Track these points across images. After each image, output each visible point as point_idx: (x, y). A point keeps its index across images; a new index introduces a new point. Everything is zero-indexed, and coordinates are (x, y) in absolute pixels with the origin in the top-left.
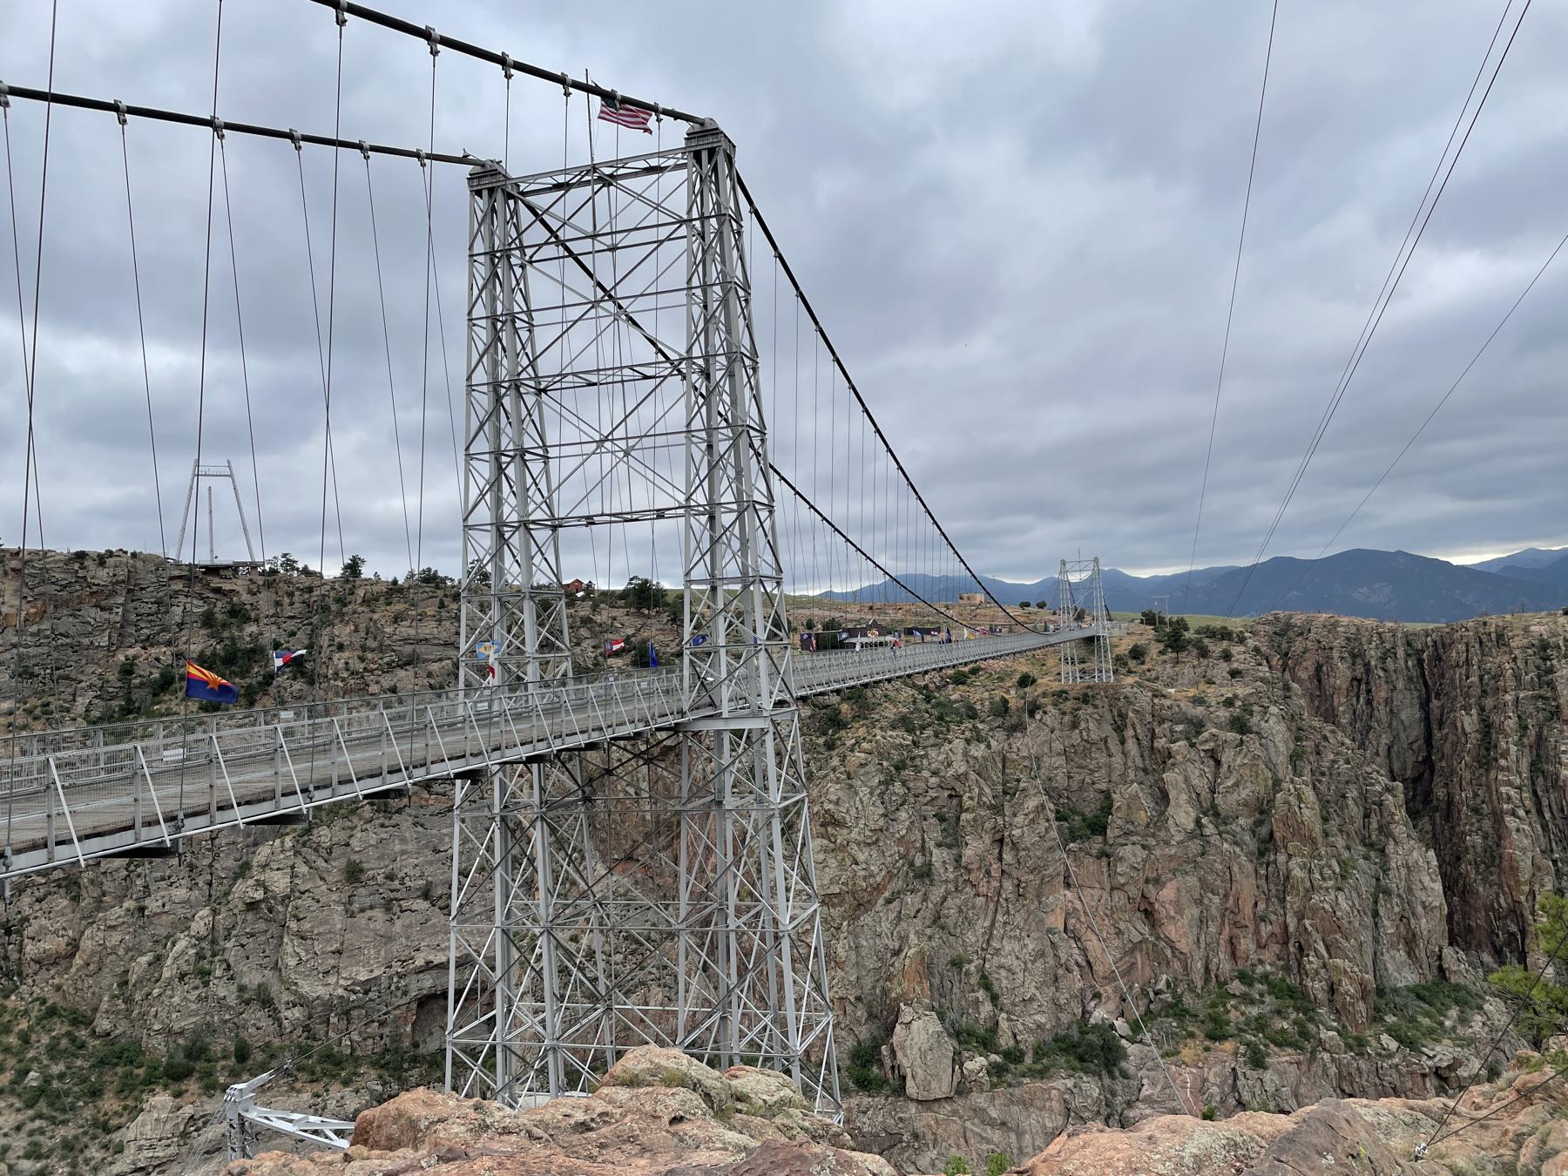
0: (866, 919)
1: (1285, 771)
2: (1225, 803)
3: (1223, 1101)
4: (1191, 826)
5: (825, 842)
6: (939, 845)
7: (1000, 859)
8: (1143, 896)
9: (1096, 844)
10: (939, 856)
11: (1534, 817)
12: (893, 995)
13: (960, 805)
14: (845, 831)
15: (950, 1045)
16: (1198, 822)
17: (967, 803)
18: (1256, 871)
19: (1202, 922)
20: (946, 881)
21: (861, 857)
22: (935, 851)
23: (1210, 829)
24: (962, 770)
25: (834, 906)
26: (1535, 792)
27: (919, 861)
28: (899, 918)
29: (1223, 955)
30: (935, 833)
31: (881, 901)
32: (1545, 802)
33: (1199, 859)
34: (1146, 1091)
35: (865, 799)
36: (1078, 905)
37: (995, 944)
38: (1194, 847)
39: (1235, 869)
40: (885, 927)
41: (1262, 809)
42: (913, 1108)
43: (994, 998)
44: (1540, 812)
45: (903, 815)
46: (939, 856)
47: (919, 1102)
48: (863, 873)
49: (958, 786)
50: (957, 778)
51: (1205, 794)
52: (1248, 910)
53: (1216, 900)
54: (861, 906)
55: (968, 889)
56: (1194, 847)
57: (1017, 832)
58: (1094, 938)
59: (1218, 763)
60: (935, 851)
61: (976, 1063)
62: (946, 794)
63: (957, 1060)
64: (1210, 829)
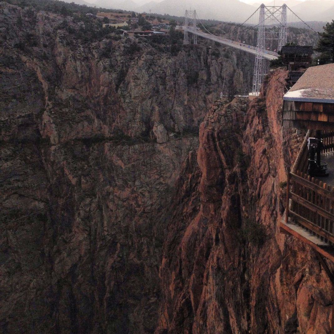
0: (144, 103)
1: (236, 68)
2: (224, 75)
4: (216, 80)
6: (161, 85)
9: (195, 85)
10: (161, 87)
12: (153, 120)
13: (165, 74)
15: (166, 131)
17: (167, 74)
23: (220, 82)
27: (156, 88)
28: (152, 102)
30: (159, 82)
40: (149, 104)
42: (158, 145)
43: (174, 121)
46: (161, 87)
47: (160, 144)
49: (165, 70)
50: (165, 68)
51: (219, 73)
54: (144, 99)
59: (222, 65)
61: (172, 135)
63: (168, 134)
64: (220, 82)
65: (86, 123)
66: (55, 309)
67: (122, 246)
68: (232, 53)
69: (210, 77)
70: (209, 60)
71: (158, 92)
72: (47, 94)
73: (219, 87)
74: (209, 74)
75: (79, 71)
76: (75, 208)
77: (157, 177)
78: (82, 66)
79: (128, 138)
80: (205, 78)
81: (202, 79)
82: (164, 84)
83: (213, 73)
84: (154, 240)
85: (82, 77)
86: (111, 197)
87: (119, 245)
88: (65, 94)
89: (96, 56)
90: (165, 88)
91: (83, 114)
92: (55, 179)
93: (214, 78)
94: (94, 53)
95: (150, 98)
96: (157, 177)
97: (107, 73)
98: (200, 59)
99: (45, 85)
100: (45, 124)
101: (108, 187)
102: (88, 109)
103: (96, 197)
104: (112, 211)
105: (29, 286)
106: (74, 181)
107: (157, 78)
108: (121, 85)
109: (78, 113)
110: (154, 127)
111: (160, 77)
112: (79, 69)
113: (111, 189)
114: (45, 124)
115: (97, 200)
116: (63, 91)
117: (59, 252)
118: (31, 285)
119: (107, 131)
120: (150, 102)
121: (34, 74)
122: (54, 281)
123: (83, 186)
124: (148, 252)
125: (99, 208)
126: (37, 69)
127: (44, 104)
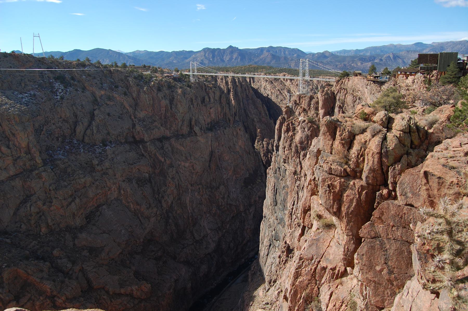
4: (213, 101)
16: (214, 101)
23: (215, 102)
38: (214, 104)
46: (192, 106)
56: (214, 104)
64: (215, 102)
65: (157, 130)
66: (168, 225)
67: (191, 190)
70: (207, 90)
72: (132, 115)
73: (215, 105)
74: (209, 98)
76: (166, 174)
77: (200, 154)
78: (149, 97)
79: (182, 135)
80: (208, 100)
81: (207, 101)
82: (192, 104)
83: (211, 97)
84: (204, 186)
85: (149, 103)
86: (180, 167)
87: (190, 190)
88: (142, 115)
89: (155, 91)
91: (154, 125)
92: (152, 160)
93: (212, 100)
96: (200, 154)
97: (164, 100)
98: (203, 89)
99: (130, 110)
100: (138, 131)
101: (178, 162)
102: (155, 122)
103: (174, 167)
104: (183, 173)
105: (156, 214)
106: (163, 160)
107: (188, 101)
108: (173, 106)
110: (194, 128)
111: (190, 101)
113: (180, 163)
114: (138, 131)
115: (175, 168)
116: (140, 113)
117: (163, 197)
118: (158, 213)
119: (168, 133)
121: (122, 104)
122: (164, 211)
123: (167, 162)
124: (203, 192)
125: (177, 172)
126: (123, 101)
127: (133, 121)
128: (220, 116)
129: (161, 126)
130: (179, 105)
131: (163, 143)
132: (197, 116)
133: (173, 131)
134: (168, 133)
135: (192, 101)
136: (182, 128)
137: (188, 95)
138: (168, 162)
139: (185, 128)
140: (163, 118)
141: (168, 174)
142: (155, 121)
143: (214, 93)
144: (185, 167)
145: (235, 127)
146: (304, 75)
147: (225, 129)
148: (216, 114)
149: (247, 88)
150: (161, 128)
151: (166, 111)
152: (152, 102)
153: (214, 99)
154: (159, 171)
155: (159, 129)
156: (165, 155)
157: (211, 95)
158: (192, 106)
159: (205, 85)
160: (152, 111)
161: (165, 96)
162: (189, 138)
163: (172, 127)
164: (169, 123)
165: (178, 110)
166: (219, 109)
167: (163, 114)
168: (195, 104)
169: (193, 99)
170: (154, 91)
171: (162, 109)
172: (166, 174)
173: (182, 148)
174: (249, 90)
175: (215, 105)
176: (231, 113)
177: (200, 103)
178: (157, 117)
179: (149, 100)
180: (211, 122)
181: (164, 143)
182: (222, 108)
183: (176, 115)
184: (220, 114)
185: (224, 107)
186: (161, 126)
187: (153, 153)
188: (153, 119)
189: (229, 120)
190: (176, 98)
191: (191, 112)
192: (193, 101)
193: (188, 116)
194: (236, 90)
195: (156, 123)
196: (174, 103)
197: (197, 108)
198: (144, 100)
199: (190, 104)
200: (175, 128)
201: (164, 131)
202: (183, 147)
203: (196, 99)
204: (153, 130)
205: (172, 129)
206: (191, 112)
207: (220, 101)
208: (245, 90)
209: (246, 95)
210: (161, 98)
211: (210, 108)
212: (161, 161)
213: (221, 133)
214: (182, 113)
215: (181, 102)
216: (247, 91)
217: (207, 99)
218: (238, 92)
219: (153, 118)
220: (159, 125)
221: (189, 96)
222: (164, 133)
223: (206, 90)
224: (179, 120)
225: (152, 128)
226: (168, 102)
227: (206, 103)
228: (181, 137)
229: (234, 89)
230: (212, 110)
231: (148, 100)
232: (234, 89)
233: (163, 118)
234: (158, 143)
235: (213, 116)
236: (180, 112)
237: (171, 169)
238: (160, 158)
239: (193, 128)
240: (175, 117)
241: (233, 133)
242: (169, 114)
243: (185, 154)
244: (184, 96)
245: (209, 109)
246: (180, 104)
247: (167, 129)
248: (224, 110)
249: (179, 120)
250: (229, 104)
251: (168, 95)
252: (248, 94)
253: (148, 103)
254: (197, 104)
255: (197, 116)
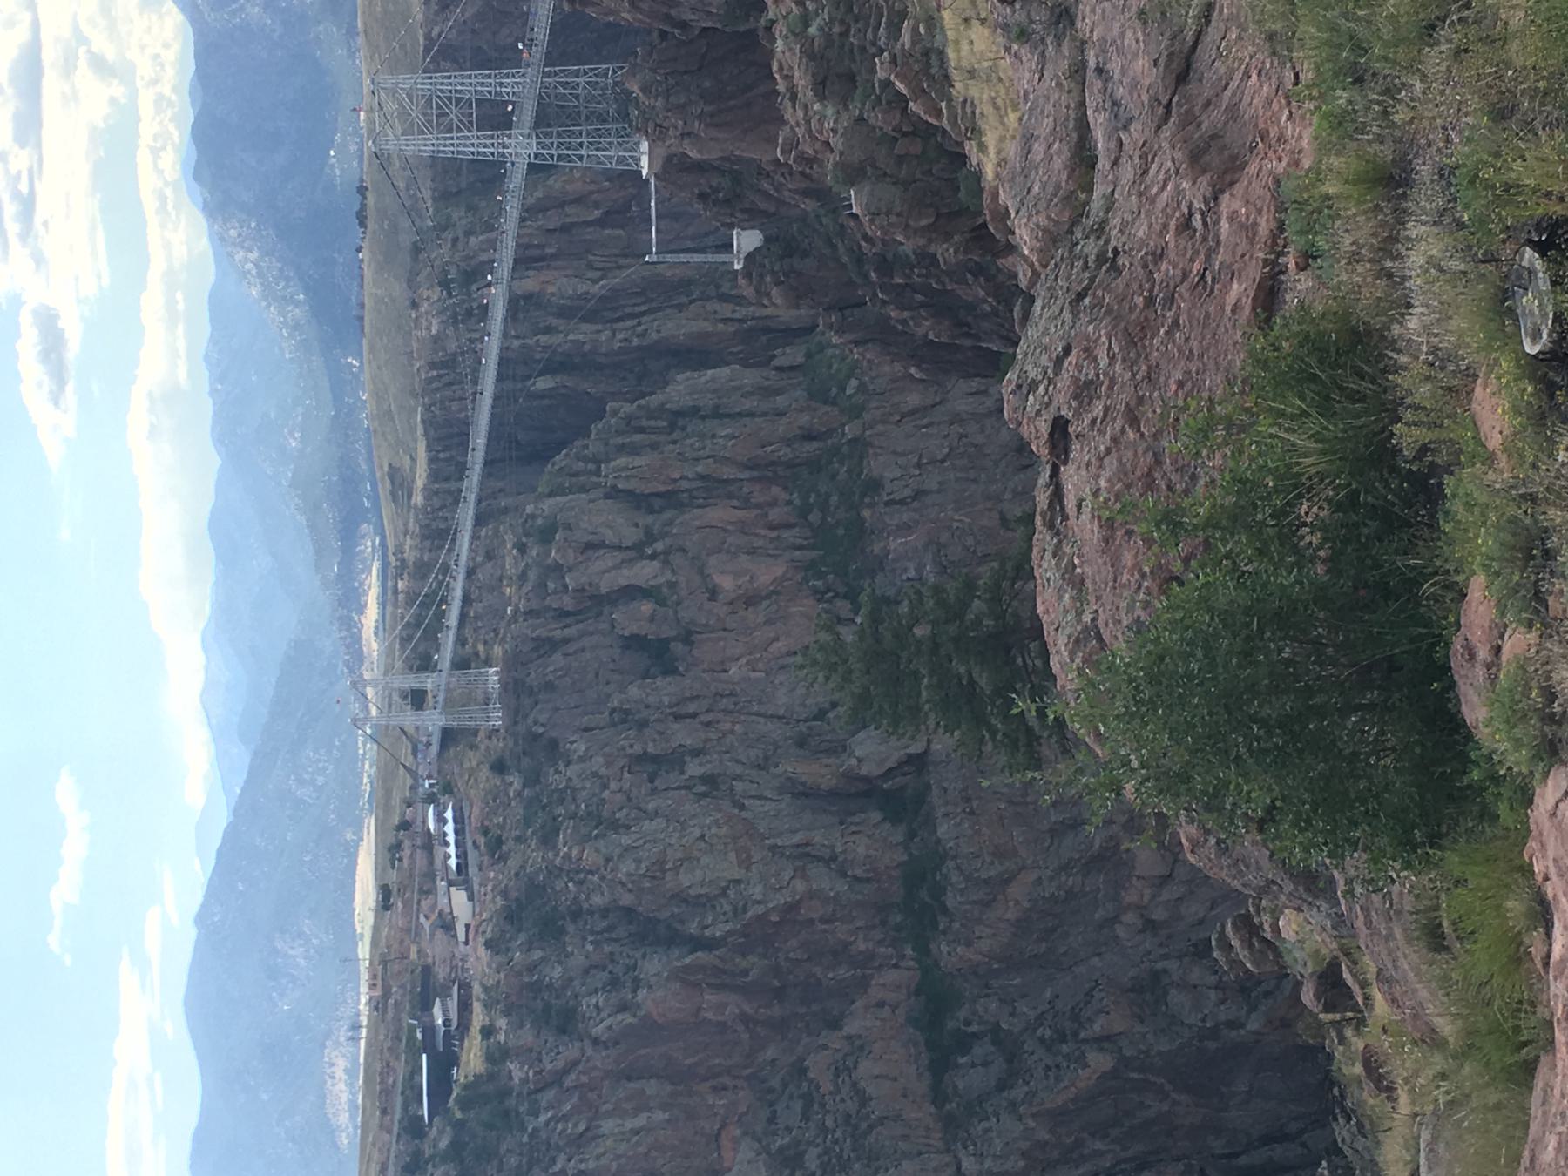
2: (631, 536)
3: (915, 510)
5: (682, 871)
6: (682, 773)
7: (694, 716)
8: (731, 603)
9: (678, 648)
11: (644, 319)
14: (669, 851)
16: (653, 557)
18: (699, 507)
19: (752, 552)
20: (721, 761)
21: (697, 833)
22: (689, 773)
24: (601, 760)
25: (749, 857)
26: (620, 319)
29: (786, 534)
31: (744, 814)
32: (628, 310)
33: (690, 554)
34: (912, 574)
35: (634, 837)
36: (743, 661)
37: (781, 712)
38: (677, 559)
39: (697, 523)
41: (639, 501)
44: (644, 313)
45: (651, 806)
46: (694, 769)
48: (713, 830)
52: (740, 514)
53: (730, 539)
55: (728, 741)
56: (677, 559)
57: (666, 700)
58: (776, 645)
60: (689, 773)
62: (626, 775)
64: (659, 546)
65: (866, 1067)
68: (533, 517)
69: (639, 589)
70: (567, 602)
71: (710, 780)
73: (683, 550)
74: (631, 593)
75: (641, 1120)
80: (647, 607)
81: (652, 619)
82: (674, 759)
83: (625, 577)
86: (1159, 914)
90: (697, 753)
91: (827, 1086)
92: (1099, 1145)
93: (645, 572)
94: (560, 1064)
95: (742, 807)
98: (566, 641)
101: (1120, 931)
102: (803, 1071)
103: (1165, 971)
106: (1099, 1062)
107: (654, 791)
108: (693, 928)
109: (823, 1105)
110: (864, 771)
111: (651, 781)
112: (629, 1124)
113: (1130, 918)
115: (1172, 965)
120: (758, 802)
123: (1118, 1028)
128: (775, 515)
129: (835, 1025)
130: (685, 879)
131: (974, 1028)
132: (774, 730)
133: (880, 942)
134: (891, 976)
135: (655, 759)
136: (859, 872)
137: (605, 787)
138: (1112, 1019)
139: (861, 848)
140: (777, 1011)
141: (1214, 1033)
142: (800, 1071)
143: (590, 546)
144: (1166, 879)
145: (862, 388)
146: (495, 117)
147: (875, 485)
148: (759, 543)
149: (553, 220)
150: (852, 1027)
151: (721, 987)
152: (652, 1087)
153: (638, 551)
154: (1183, 1098)
155: (859, 1046)
156: (1063, 1040)
157: (607, 574)
158: (694, 769)
159: (529, 613)
160: (725, 1088)
161: (614, 983)
162: (943, 830)
163: (846, 945)
164: (818, 970)
165: (724, 892)
166: (719, 514)
167: (748, 1009)
168: (683, 735)
169: (638, 749)
170: (575, 1063)
171: (710, 1015)
172: (1212, 1045)
173: (1015, 890)
174: (562, 205)
175: (683, 550)
176: (748, 404)
177: (665, 689)
178: (770, 1053)
179: (637, 1111)
180: (819, 595)
181: (968, 1023)
182: (712, 488)
183: (760, 909)
184: (758, 506)
185: (702, 477)
186: (835, 1025)
187: (1043, 1135)
188: (785, 1085)
189: (809, 436)
190: (627, 900)
191: (738, 778)
192: (651, 749)
193: (768, 806)
194: (565, 313)
195: (818, 1067)
196: (664, 914)
197: (708, 724)
198: (641, 1150)
199: (674, 779)
200: (859, 924)
201: (881, 1004)
202: (1008, 881)
203: (643, 725)
204: (864, 1100)
205: (862, 946)
206: (738, 778)
207: (657, 503)
208: (565, 229)
209: (601, 223)
210: (627, 1018)
211: (713, 594)
212: (1114, 1074)
213: (906, 528)
214: (746, 864)
215: (660, 863)
216: (574, 214)
217: (636, 618)
218: (585, 296)
219: (775, 1083)
220: (835, 1040)
221: (613, 785)
222: (894, 1008)
223: (568, 614)
224: (800, 886)
225: (851, 1106)
226: (654, 965)
227: (668, 632)
228: (924, 894)
229: (554, 321)
230: (726, 583)
231: (641, 1120)
232: (554, 321)
233: (777, 1011)
234: (971, 1078)
235: (768, 573)
236: (738, 873)
237: (1176, 998)
238: (1085, 1078)
239: (866, 779)
240: (774, 918)
241: (913, 412)
242: (755, 965)
243: (1065, 868)
244: (615, 826)
245: (720, 609)
246: (676, 869)
247: (863, 984)
248: (728, 472)
249: (800, 886)
250: (679, 414)
251: (607, 948)
252: (597, 213)
253: (660, 1116)
254: (678, 717)
255: (774, 730)
